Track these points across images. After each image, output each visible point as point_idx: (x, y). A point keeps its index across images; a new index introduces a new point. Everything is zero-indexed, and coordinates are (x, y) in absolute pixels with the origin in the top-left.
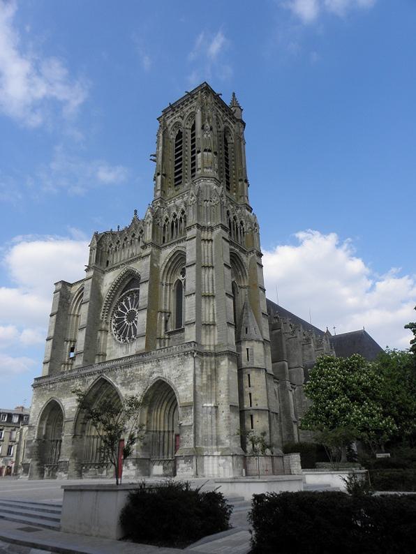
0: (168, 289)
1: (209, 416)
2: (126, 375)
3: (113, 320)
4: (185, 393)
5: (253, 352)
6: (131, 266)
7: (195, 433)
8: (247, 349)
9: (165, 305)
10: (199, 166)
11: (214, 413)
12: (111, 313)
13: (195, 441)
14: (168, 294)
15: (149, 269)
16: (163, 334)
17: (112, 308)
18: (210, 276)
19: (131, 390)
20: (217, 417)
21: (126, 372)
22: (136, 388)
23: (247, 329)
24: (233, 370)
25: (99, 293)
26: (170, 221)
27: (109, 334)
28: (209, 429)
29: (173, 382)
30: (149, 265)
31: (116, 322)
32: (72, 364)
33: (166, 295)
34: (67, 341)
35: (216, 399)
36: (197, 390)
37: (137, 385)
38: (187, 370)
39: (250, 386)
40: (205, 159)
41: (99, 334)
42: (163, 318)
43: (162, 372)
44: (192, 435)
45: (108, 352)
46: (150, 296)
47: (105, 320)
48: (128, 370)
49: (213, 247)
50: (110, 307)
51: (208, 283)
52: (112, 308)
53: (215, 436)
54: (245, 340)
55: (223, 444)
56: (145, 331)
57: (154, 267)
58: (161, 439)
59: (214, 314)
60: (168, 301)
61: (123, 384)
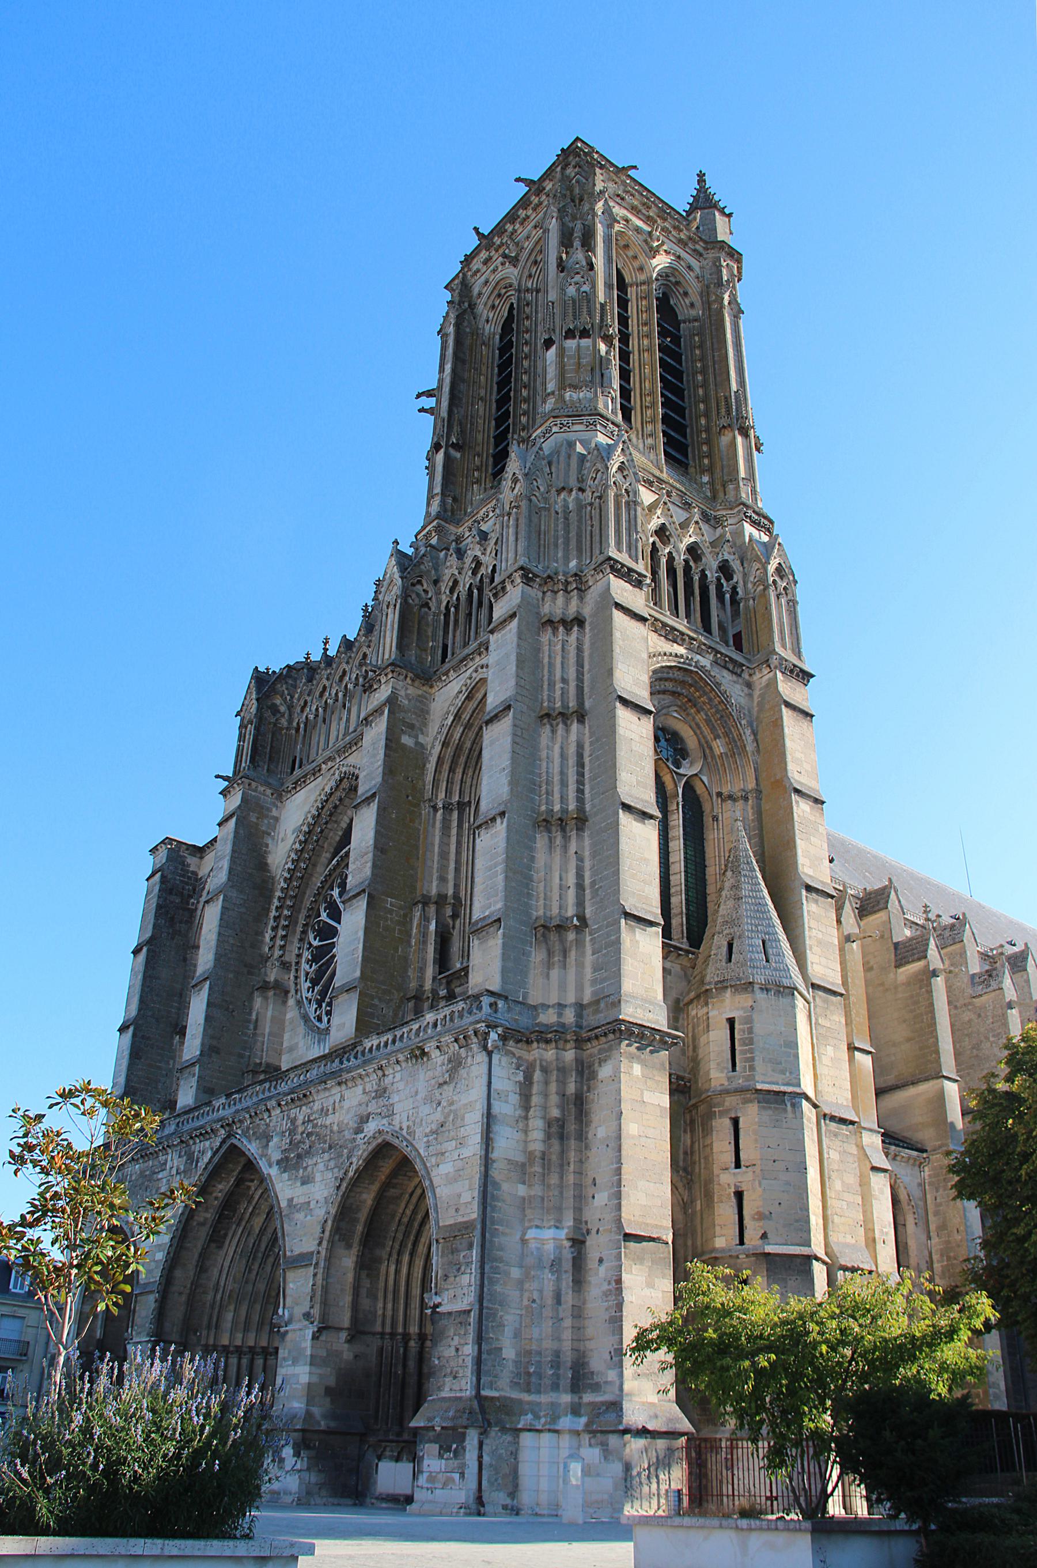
0: (455, 823)
1: (548, 1277)
3: (307, 955)
5: (750, 1030)
7: (480, 1339)
8: (731, 1022)
9: (443, 879)
10: (551, 386)
11: (567, 1265)
13: (478, 1373)
14: (454, 839)
15: (382, 752)
16: (428, 985)
17: (303, 913)
18: (572, 749)
19: (303, 1184)
20: (579, 1282)
21: (293, 1121)
22: (318, 1177)
23: (730, 946)
24: (648, 1097)
25: (263, 866)
26: (462, 589)
27: (291, 1002)
28: (547, 1326)
29: (421, 1146)
30: (383, 743)
31: (315, 959)
33: (445, 844)
35: (578, 1210)
36: (495, 1174)
37: (321, 1166)
38: (464, 1099)
39: (738, 1165)
40: (570, 365)
41: (258, 1002)
42: (433, 927)
44: (469, 1350)
46: (380, 848)
47: (277, 953)
49: (586, 646)
50: (295, 909)
51: (563, 773)
52: (303, 913)
53: (568, 1357)
54: (722, 986)
55: (596, 1388)
56: (358, 974)
57: (404, 747)
58: (412, 1364)
59: (580, 887)
60: (452, 865)
61: (284, 1164)
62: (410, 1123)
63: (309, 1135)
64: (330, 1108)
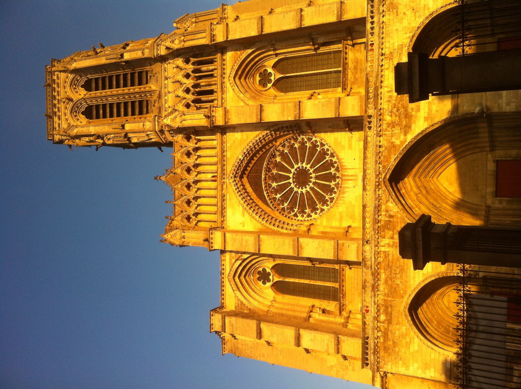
6: (228, 172)
12: (287, 220)
34: (310, 316)
43: (401, 47)
45: (345, 224)
48: (388, 118)
61: (407, 129)
62: (408, 31)
63: (398, 110)
64: (390, 94)
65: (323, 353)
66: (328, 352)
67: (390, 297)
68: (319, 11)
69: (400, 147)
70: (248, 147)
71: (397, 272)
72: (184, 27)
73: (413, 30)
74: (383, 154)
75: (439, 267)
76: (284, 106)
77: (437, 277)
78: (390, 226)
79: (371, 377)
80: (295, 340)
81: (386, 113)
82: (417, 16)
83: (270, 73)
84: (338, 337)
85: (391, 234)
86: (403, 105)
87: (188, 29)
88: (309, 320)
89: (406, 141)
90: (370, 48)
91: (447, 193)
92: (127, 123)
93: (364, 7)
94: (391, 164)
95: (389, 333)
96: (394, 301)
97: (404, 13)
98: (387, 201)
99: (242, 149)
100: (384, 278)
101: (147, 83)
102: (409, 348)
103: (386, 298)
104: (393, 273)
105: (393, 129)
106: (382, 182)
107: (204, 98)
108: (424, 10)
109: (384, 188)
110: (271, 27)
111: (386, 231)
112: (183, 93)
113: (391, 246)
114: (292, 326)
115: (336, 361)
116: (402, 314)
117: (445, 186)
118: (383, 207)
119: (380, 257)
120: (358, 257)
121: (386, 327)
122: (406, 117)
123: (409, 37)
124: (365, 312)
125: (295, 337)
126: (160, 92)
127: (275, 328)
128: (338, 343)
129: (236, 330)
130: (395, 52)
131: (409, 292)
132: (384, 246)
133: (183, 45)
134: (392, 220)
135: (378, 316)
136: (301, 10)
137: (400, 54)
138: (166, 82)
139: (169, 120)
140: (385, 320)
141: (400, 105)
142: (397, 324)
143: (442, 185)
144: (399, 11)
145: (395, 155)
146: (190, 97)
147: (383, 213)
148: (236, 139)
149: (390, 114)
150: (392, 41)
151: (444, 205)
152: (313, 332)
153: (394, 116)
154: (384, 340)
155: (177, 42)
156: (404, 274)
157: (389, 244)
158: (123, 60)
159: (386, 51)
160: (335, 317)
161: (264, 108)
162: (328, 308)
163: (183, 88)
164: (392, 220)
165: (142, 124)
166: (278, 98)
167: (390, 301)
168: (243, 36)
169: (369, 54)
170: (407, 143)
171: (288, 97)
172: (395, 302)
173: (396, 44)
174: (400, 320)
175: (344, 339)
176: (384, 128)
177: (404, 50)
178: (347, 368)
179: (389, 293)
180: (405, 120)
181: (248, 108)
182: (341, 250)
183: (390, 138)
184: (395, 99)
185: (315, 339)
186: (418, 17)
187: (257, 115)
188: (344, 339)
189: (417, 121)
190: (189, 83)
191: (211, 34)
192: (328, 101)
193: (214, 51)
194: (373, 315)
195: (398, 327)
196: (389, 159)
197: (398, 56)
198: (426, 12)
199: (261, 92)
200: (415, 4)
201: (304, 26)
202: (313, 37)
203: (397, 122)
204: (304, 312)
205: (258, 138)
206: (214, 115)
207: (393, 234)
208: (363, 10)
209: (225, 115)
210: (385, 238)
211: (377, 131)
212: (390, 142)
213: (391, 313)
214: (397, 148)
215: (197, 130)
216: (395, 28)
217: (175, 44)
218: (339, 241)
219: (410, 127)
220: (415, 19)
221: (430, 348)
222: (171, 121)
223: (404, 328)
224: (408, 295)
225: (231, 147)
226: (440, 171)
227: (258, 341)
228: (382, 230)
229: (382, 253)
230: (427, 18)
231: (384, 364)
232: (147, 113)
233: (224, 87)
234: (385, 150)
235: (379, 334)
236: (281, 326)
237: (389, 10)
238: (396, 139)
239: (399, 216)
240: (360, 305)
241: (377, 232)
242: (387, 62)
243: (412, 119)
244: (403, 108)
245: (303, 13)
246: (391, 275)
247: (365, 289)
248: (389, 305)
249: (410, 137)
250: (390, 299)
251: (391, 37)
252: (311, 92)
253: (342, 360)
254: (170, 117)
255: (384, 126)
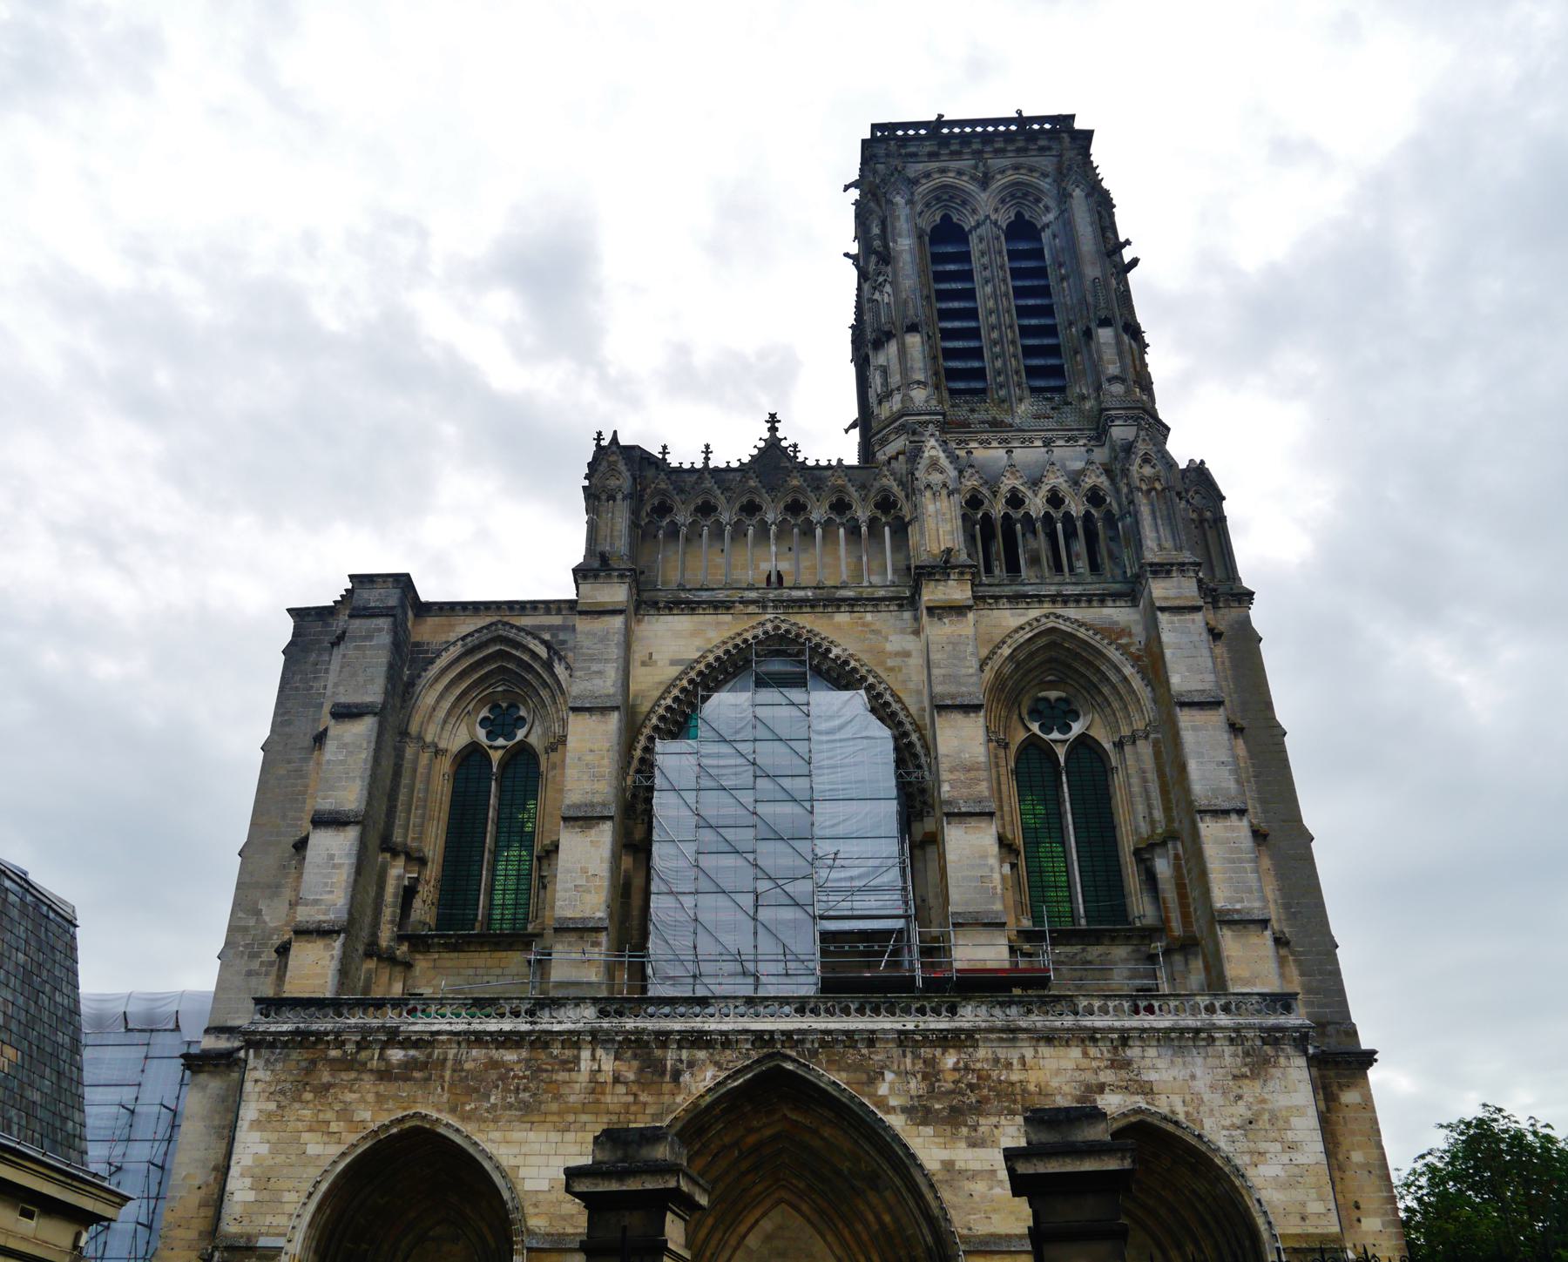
2: (931, 1073)
4: (1298, 1195)
19: (973, 1144)
21: (931, 1063)
32: (408, 966)
34: (395, 854)
43: (1147, 1090)
48: (950, 1060)
61: (920, 1113)
62: (1190, 1109)
63: (971, 1086)
64: (1015, 1062)
65: (296, 890)
66: (297, 904)
67: (452, 1077)
68: (1241, 861)
69: (870, 1096)
70: (863, 671)
71: (525, 1096)
72: (1187, 491)
73: (1193, 1121)
74: (851, 1051)
75: (537, 1210)
76: (977, 770)
77: (510, 1205)
78: (650, 1076)
79: (231, 1023)
80: (330, 812)
81: (963, 1056)
82: (1234, 1133)
83: (1070, 728)
84: (338, 933)
85: (626, 1077)
86: (986, 1100)
87: (1183, 502)
88: (384, 850)
89: (888, 1112)
90: (1142, 1004)
91: (743, 1229)
92: (922, 337)
93: (1255, 985)
94: (821, 1072)
95: (353, 1075)
96: (443, 1088)
97: (1240, 1097)
98: (718, 1065)
99: (860, 655)
100: (505, 1058)
101: (1033, 390)
102: (310, 1130)
103: (449, 1064)
104: (518, 1085)
105: (919, 1076)
106: (771, 1051)
107: (998, 545)
108: (1251, 1153)
109: (754, 1055)
110: (1195, 729)
111: (635, 1064)
112: (1010, 491)
113: (595, 1075)
114: (369, 803)
115: (272, 925)
116: (405, 1109)
117: (761, 1223)
118: (702, 1055)
119: (563, 1048)
120: (560, 985)
121: (369, 1066)
122: (953, 1109)
123: (1173, 1112)
124: (410, 1007)
125: (337, 812)
126: (1011, 426)
127: (363, 756)
128: (323, 932)
129: (357, 648)
130: (1131, 1075)
131: (467, 1128)
132: (593, 1058)
133: (1139, 489)
134: (668, 1078)
135: (399, 1042)
136: (1241, 812)
137: (1126, 1088)
138: (1038, 443)
139: (933, 453)
140: (388, 1062)
141: (985, 1092)
142: (377, 1094)
143: (764, 1214)
144: (1247, 1081)
145: (847, 1084)
146: (998, 509)
147: (685, 1054)
148: (886, 638)
149: (961, 1065)
150: (1160, 1063)
151: (710, 1221)
152: (353, 860)
153: (957, 1076)
154: (334, 1060)
155: (1147, 471)
156: (517, 1113)
157: (599, 1070)
158: (1093, 325)
159: (1133, 1052)
160: (392, 922)
161: (972, 715)
162: (417, 903)
163: (1021, 488)
164: (668, 1078)
165: (921, 377)
166: (1002, 753)
167: (442, 1077)
168: (1168, 653)
169: (1124, 1003)
170: (880, 1115)
171: (1003, 779)
172: (439, 1090)
173: (1152, 1076)
174: (390, 1105)
175: (334, 948)
176: (922, 1050)
177: (1138, 1098)
178: (254, 956)
179: (464, 1074)
180: (944, 1108)
181: (971, 671)
182: (582, 938)
183: (896, 1068)
184: (1002, 1078)
185: (335, 866)
186: (1231, 1136)
187: (953, 697)
188: (334, 948)
189: (941, 1140)
190: (1036, 505)
191: (1172, 565)
192: (995, 894)
193: (1125, 572)
194: (401, 1029)
195: (371, 1098)
196: (836, 1068)
197: (1122, 1084)
198: (1246, 1158)
199: (1016, 705)
200: (1268, 1127)
201: (1199, 819)
202: (1170, 846)
203: (939, 1087)
204: (406, 835)
205: (888, 697)
206: (952, 577)
207: (626, 1083)
208: (1246, 983)
209: (951, 608)
210: (616, 1059)
211: (913, 1032)
212: (882, 1068)
213: (407, 1079)
214: (866, 1089)
215: (910, 529)
216: (1199, 1073)
217: (1141, 467)
218: (604, 933)
219: (925, 1122)
220: (1224, 1128)
221: (311, 1190)
222: (931, 457)
223: (367, 1115)
224: (457, 1125)
225: (864, 625)
226: (804, 1207)
227: (326, 709)
228: (639, 1051)
229: (576, 1052)
230: (1228, 1160)
231: (267, 1061)
232: (953, 392)
233: (1028, 603)
234: (862, 1055)
235: (350, 1048)
236: (368, 773)
237: (1247, 1054)
238: (892, 1083)
239: (679, 1099)
240: (427, 991)
241: (633, 1038)
242: (1105, 1053)
243: (948, 1128)
244: (978, 1102)
245: (1234, 817)
246: (513, 1078)
247: (473, 1005)
248: (431, 1075)
249: (896, 1122)
250: (448, 1074)
251: (1172, 1062)
252: (1019, 842)
253: (276, 941)
254: (942, 455)
255: (926, 1052)
